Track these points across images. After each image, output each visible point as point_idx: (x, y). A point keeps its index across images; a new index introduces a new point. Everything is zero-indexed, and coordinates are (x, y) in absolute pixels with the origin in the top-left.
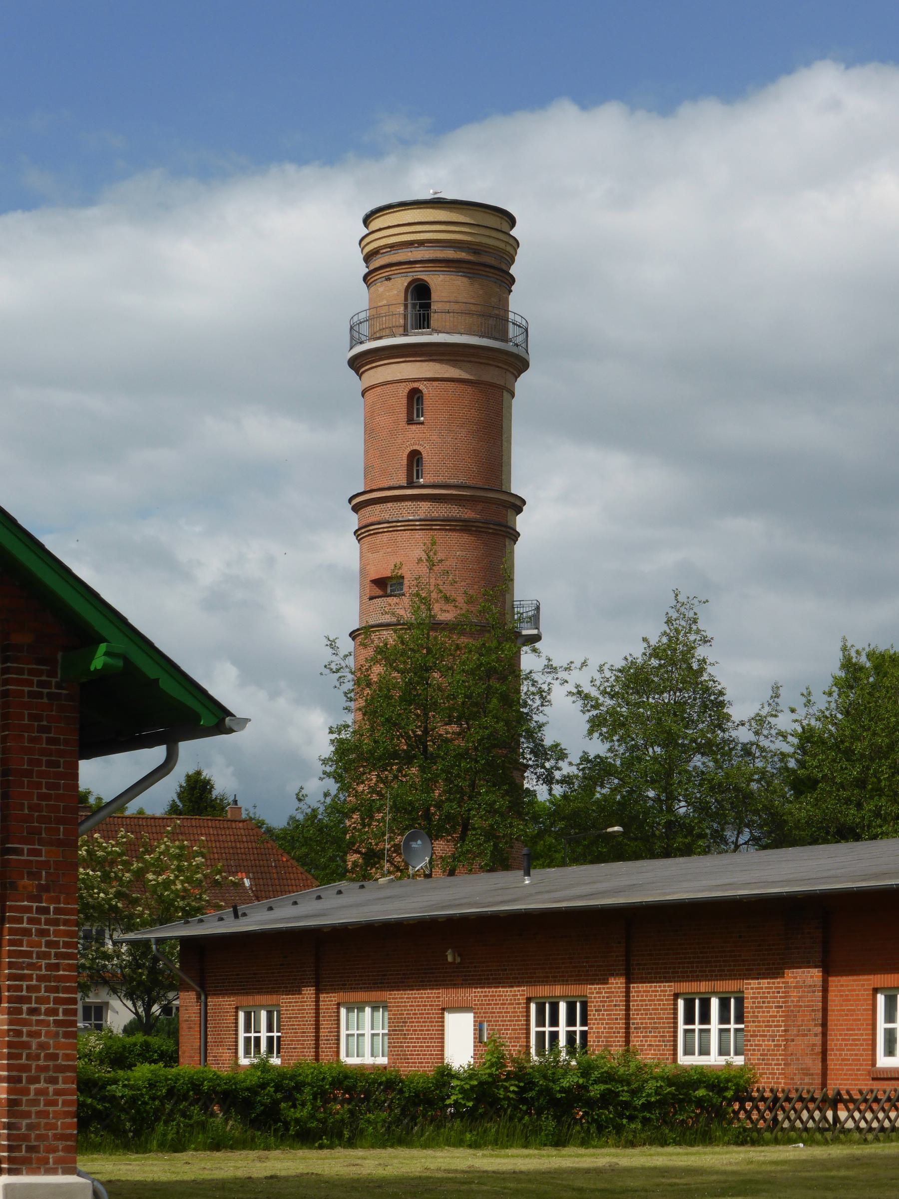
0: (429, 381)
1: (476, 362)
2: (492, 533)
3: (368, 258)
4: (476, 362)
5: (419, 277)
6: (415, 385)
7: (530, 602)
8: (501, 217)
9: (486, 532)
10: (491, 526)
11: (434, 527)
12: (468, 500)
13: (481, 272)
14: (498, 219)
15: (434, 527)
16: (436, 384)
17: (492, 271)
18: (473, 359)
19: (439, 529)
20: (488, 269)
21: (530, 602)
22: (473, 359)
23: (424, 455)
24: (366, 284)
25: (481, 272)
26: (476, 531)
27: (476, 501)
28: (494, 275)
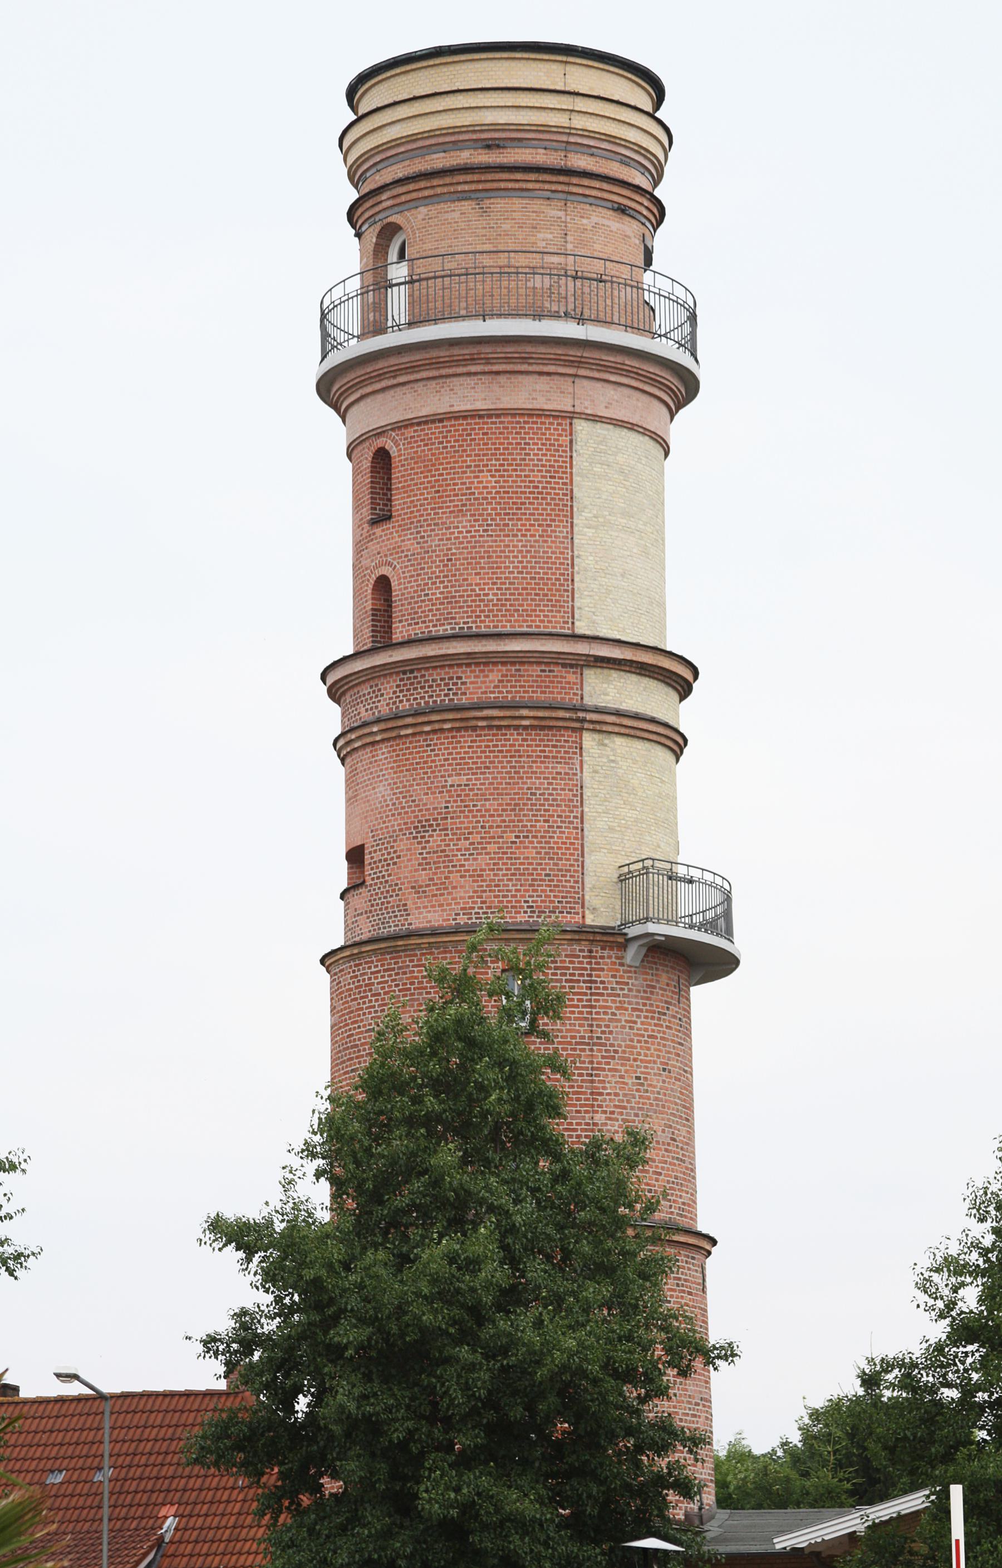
0: (399, 428)
1: (484, 373)
2: (533, 727)
3: (355, 177)
4: (484, 373)
5: (390, 220)
6: (380, 442)
7: (640, 865)
8: (561, 62)
9: (517, 727)
10: (525, 712)
11: (403, 732)
12: (468, 665)
13: (502, 185)
14: (554, 66)
15: (403, 732)
16: (410, 432)
17: (533, 176)
18: (473, 369)
19: (414, 734)
20: (519, 176)
21: (640, 865)
22: (473, 369)
23: (394, 584)
24: (353, 226)
25: (502, 185)
26: (490, 727)
27: (486, 664)
28: (537, 186)
